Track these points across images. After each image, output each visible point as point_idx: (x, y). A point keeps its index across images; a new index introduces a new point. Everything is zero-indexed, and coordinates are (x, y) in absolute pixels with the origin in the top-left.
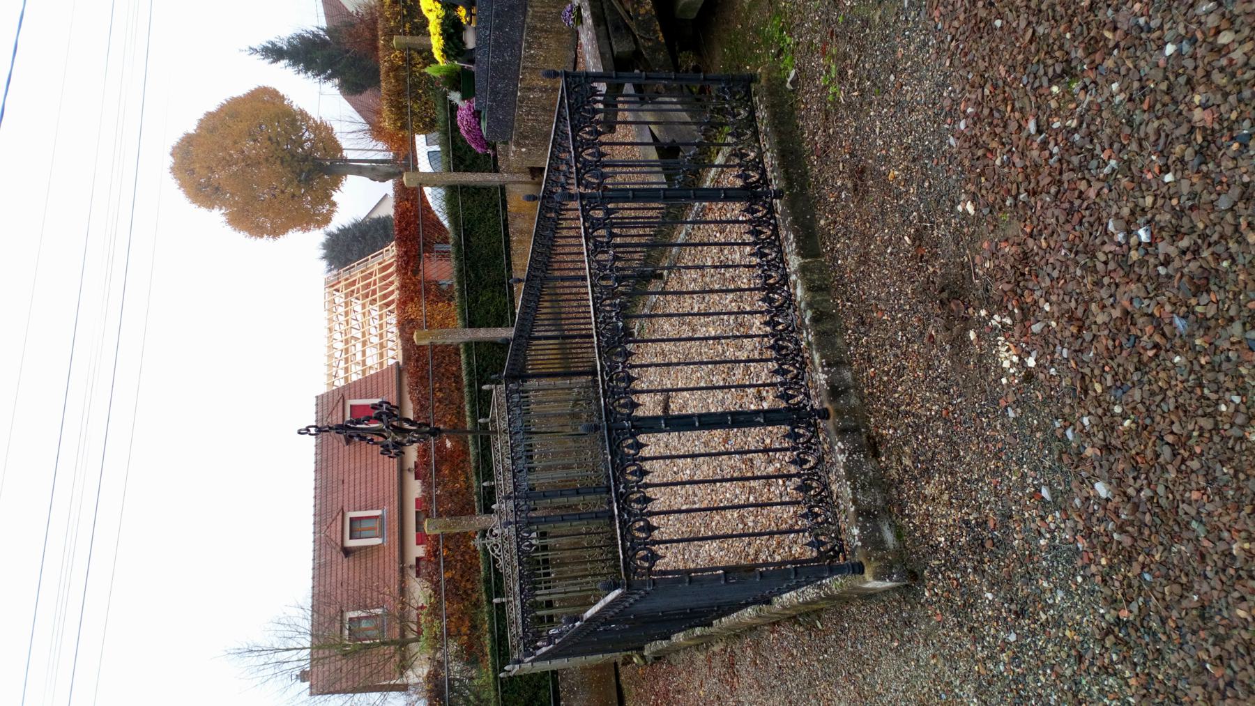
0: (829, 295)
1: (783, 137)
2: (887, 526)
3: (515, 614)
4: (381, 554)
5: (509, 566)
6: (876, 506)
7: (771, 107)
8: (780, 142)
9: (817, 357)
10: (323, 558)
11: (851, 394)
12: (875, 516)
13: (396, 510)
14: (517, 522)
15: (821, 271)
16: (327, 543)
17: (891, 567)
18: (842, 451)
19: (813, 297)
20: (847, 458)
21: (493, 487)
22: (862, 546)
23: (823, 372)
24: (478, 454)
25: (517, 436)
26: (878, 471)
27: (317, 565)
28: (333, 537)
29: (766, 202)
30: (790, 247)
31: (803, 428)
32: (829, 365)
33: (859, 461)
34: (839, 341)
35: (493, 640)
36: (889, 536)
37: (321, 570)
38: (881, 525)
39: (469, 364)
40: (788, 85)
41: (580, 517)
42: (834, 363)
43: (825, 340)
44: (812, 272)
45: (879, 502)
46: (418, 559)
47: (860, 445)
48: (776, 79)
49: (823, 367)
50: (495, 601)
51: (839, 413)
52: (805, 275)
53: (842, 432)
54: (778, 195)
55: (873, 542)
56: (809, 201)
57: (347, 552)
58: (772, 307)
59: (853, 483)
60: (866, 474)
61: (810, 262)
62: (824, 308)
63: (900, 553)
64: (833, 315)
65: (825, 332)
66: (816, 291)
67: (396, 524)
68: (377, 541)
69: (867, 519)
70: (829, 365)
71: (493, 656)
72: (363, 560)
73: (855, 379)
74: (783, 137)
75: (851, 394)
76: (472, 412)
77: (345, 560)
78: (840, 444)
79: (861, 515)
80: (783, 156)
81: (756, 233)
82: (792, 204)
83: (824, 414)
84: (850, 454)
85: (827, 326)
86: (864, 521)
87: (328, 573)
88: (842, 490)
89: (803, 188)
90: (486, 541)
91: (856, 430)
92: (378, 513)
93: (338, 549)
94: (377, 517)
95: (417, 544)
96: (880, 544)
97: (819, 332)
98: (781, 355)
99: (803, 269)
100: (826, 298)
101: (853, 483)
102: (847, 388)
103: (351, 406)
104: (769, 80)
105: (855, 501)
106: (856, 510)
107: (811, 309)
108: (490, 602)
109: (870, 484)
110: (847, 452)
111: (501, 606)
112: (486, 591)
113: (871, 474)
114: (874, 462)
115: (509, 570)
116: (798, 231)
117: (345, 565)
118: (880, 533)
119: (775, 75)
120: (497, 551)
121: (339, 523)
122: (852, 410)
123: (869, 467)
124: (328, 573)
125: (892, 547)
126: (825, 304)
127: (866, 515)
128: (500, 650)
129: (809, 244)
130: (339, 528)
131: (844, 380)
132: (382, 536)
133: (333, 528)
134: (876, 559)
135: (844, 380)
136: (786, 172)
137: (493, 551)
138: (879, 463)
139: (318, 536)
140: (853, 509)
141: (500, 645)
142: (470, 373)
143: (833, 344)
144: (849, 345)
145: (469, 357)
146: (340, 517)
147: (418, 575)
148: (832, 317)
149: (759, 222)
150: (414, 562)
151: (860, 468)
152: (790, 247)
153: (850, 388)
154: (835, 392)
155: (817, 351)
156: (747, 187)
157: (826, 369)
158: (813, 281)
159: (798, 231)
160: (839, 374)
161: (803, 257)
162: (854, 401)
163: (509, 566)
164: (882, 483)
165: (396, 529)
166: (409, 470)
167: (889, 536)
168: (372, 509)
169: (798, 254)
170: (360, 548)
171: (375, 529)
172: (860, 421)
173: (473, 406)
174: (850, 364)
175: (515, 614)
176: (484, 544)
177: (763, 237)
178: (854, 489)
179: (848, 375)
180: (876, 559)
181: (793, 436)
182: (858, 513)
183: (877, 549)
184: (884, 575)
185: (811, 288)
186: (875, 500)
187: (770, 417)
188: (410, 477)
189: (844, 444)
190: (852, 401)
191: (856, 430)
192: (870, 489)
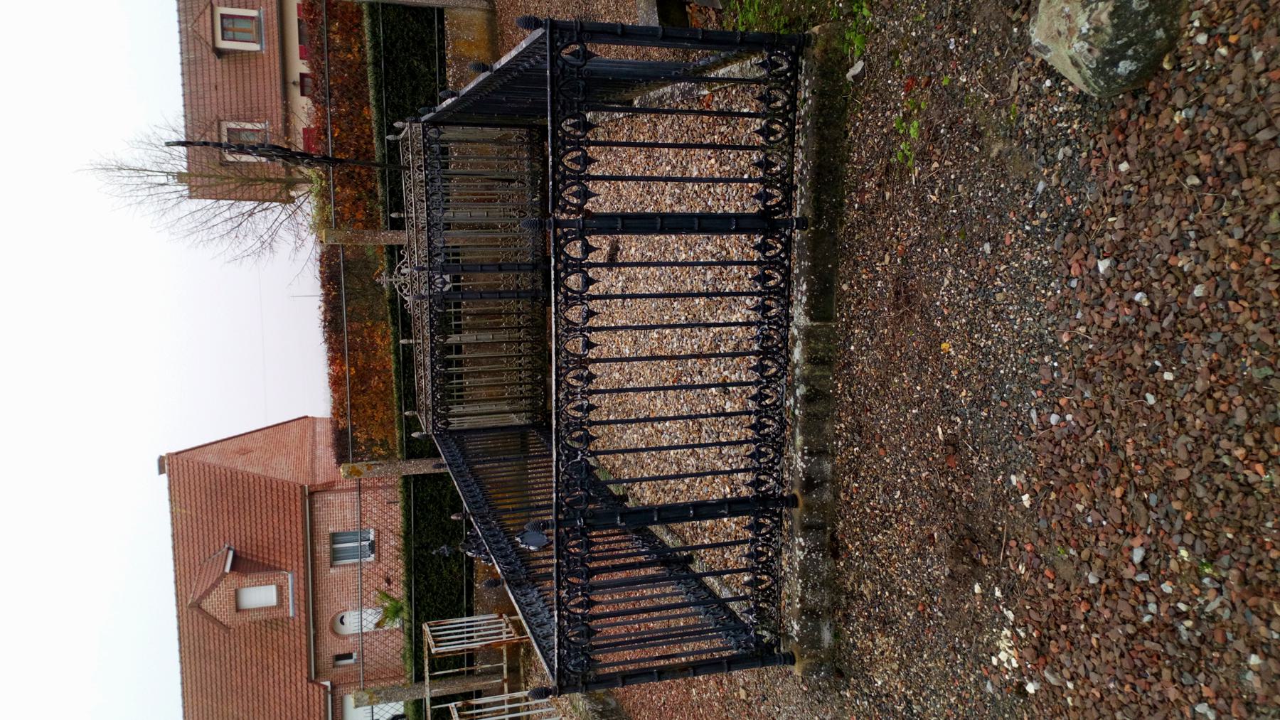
0: (830, 370)
1: (825, 146)
2: (828, 626)
3: (424, 358)
4: (260, 61)
5: (421, 314)
6: (821, 606)
7: (819, 94)
8: (820, 153)
9: (799, 440)
10: (192, 53)
11: (826, 489)
12: (818, 616)
13: (275, 15)
14: (430, 296)
15: (829, 340)
16: (195, 38)
17: (821, 665)
18: (802, 549)
19: (813, 371)
20: (805, 557)
21: (402, 220)
22: (798, 643)
23: (803, 460)
24: (384, 155)
25: (435, 198)
26: (833, 571)
27: (185, 61)
28: (202, 33)
29: (784, 235)
30: (800, 292)
31: (768, 518)
32: (810, 453)
33: (817, 560)
34: (828, 426)
35: (398, 362)
36: (827, 636)
37: (191, 69)
38: (822, 624)
39: (374, 34)
40: (849, 75)
41: (500, 295)
42: (816, 452)
43: (813, 424)
44: (817, 339)
45: (826, 603)
46: (303, 76)
47: (822, 544)
48: (835, 50)
49: (803, 454)
50: (402, 342)
51: (808, 508)
52: (809, 343)
53: (806, 528)
54: (802, 223)
55: (810, 639)
56: (835, 244)
57: (220, 53)
58: (763, 376)
59: (804, 582)
60: (819, 574)
61: (819, 326)
62: (820, 386)
63: (834, 651)
64: (829, 395)
65: (815, 415)
66: (817, 364)
67: (276, 30)
68: (255, 47)
69: (810, 618)
70: (810, 453)
71: (397, 377)
72: (239, 66)
73: (833, 472)
74: (825, 146)
75: (826, 489)
76: (377, 100)
77: (218, 61)
78: (801, 540)
79: (805, 614)
80: (818, 174)
81: (763, 279)
82: (815, 243)
83: (792, 502)
84: (809, 553)
85: (818, 408)
86: (807, 619)
87: (200, 73)
88: (794, 588)
89: (832, 225)
90: (393, 279)
91: (821, 528)
92: (254, 13)
93: (210, 49)
94: (252, 18)
95: (301, 58)
96: (815, 643)
97: (809, 414)
98: (760, 435)
99: (809, 334)
100: (827, 373)
101: (805, 582)
102: (824, 481)
103: (229, 130)
104: (825, 51)
105: (802, 600)
106: (801, 609)
107: (806, 385)
108: (382, 140)
109: (822, 584)
110: (806, 550)
111: (408, 350)
112: (391, 311)
113: (825, 574)
114: (831, 562)
115: (418, 312)
116: (814, 284)
117: (219, 66)
118: (819, 632)
119: (835, 44)
120: (405, 291)
121: (208, 18)
122: (823, 506)
123: (824, 568)
124: (200, 73)
125: (827, 646)
126: (823, 382)
127: (810, 614)
128: (404, 372)
129: (820, 307)
130: (209, 24)
131: (822, 472)
132: (259, 41)
133: (202, 24)
134: (809, 657)
135: (823, 472)
136: (817, 199)
137: (401, 291)
138: (836, 564)
139: (184, 26)
140: (798, 606)
141: (405, 367)
142: (375, 46)
143: (821, 430)
144: (838, 437)
145: (374, 25)
146: (208, 11)
147: (303, 94)
148: (827, 397)
149: (772, 263)
150: (297, 78)
151: (815, 567)
152: (800, 292)
153: (826, 481)
154: (810, 484)
155: (802, 433)
156: (766, 214)
157: (806, 458)
158: (816, 351)
159: (814, 284)
160: (819, 464)
161: (812, 319)
162: (827, 496)
163: (421, 314)
164: (833, 584)
165: (276, 37)
166: (294, 83)
167: (827, 636)
168: (246, 7)
169: (807, 313)
170: (235, 52)
171: (250, 32)
172: (828, 518)
173: (378, 92)
174: (834, 455)
175: (424, 358)
176: (391, 282)
177: (772, 283)
178: (805, 588)
179: (827, 466)
180: (809, 657)
181: (753, 527)
182: (803, 611)
183: (813, 647)
184: (813, 671)
185: (813, 360)
186: (822, 601)
187: (733, 506)
188: (296, 92)
189: (805, 541)
190: (825, 497)
191: (821, 528)
192: (820, 589)
